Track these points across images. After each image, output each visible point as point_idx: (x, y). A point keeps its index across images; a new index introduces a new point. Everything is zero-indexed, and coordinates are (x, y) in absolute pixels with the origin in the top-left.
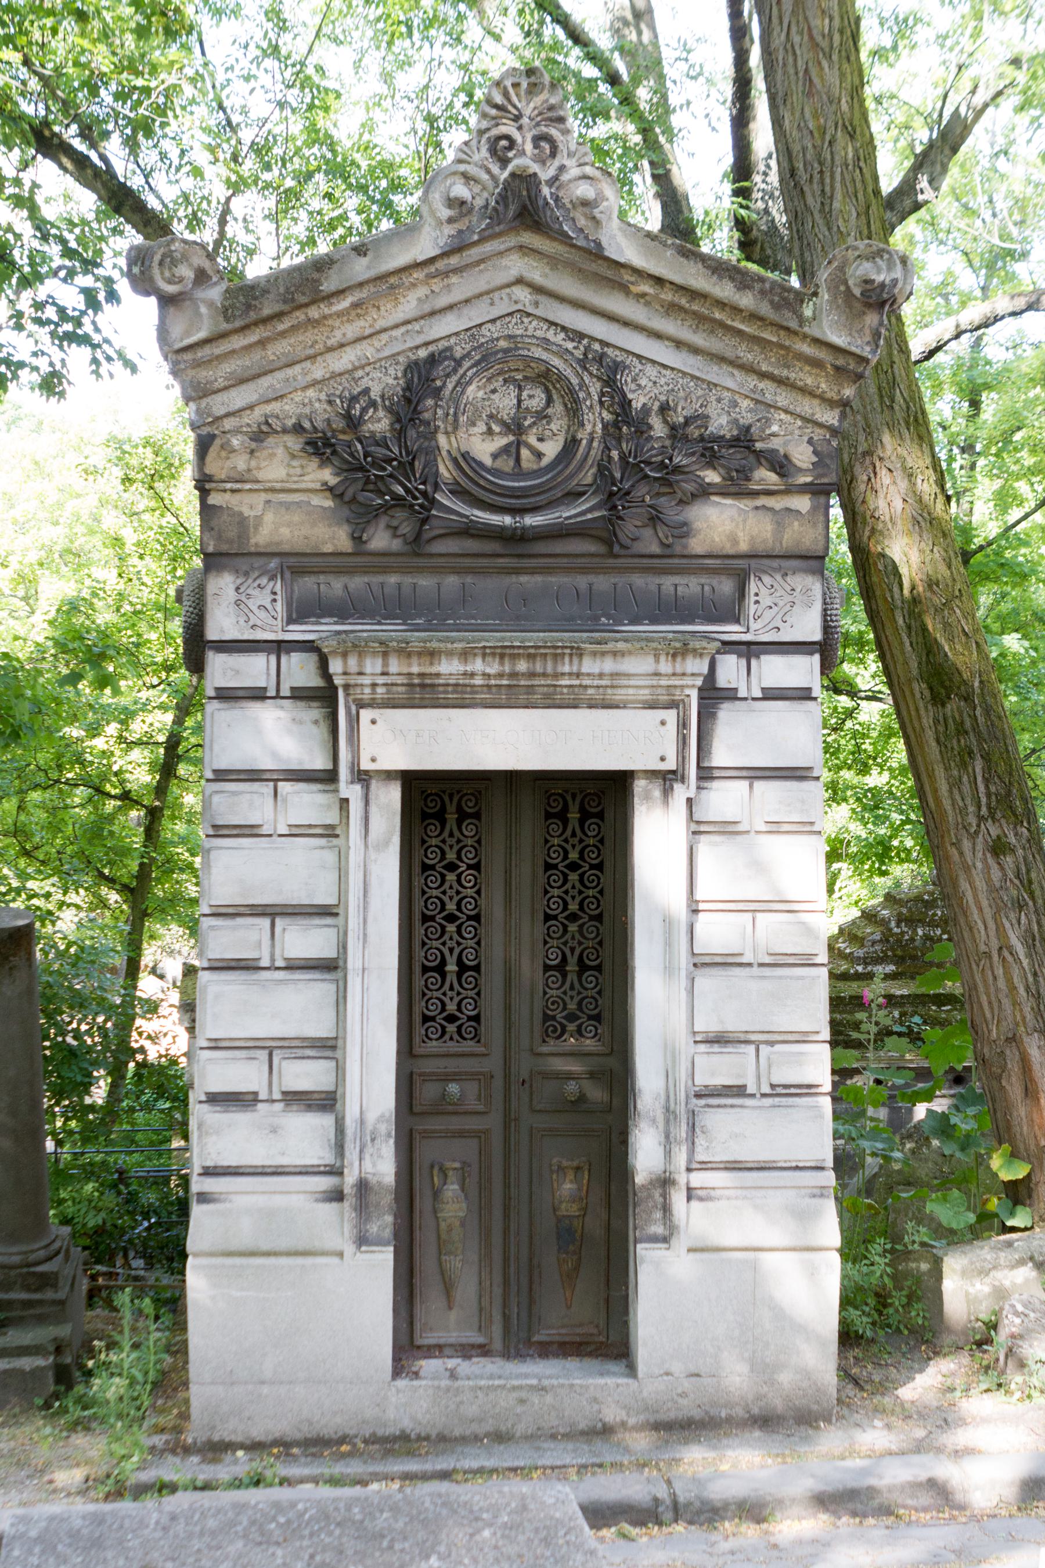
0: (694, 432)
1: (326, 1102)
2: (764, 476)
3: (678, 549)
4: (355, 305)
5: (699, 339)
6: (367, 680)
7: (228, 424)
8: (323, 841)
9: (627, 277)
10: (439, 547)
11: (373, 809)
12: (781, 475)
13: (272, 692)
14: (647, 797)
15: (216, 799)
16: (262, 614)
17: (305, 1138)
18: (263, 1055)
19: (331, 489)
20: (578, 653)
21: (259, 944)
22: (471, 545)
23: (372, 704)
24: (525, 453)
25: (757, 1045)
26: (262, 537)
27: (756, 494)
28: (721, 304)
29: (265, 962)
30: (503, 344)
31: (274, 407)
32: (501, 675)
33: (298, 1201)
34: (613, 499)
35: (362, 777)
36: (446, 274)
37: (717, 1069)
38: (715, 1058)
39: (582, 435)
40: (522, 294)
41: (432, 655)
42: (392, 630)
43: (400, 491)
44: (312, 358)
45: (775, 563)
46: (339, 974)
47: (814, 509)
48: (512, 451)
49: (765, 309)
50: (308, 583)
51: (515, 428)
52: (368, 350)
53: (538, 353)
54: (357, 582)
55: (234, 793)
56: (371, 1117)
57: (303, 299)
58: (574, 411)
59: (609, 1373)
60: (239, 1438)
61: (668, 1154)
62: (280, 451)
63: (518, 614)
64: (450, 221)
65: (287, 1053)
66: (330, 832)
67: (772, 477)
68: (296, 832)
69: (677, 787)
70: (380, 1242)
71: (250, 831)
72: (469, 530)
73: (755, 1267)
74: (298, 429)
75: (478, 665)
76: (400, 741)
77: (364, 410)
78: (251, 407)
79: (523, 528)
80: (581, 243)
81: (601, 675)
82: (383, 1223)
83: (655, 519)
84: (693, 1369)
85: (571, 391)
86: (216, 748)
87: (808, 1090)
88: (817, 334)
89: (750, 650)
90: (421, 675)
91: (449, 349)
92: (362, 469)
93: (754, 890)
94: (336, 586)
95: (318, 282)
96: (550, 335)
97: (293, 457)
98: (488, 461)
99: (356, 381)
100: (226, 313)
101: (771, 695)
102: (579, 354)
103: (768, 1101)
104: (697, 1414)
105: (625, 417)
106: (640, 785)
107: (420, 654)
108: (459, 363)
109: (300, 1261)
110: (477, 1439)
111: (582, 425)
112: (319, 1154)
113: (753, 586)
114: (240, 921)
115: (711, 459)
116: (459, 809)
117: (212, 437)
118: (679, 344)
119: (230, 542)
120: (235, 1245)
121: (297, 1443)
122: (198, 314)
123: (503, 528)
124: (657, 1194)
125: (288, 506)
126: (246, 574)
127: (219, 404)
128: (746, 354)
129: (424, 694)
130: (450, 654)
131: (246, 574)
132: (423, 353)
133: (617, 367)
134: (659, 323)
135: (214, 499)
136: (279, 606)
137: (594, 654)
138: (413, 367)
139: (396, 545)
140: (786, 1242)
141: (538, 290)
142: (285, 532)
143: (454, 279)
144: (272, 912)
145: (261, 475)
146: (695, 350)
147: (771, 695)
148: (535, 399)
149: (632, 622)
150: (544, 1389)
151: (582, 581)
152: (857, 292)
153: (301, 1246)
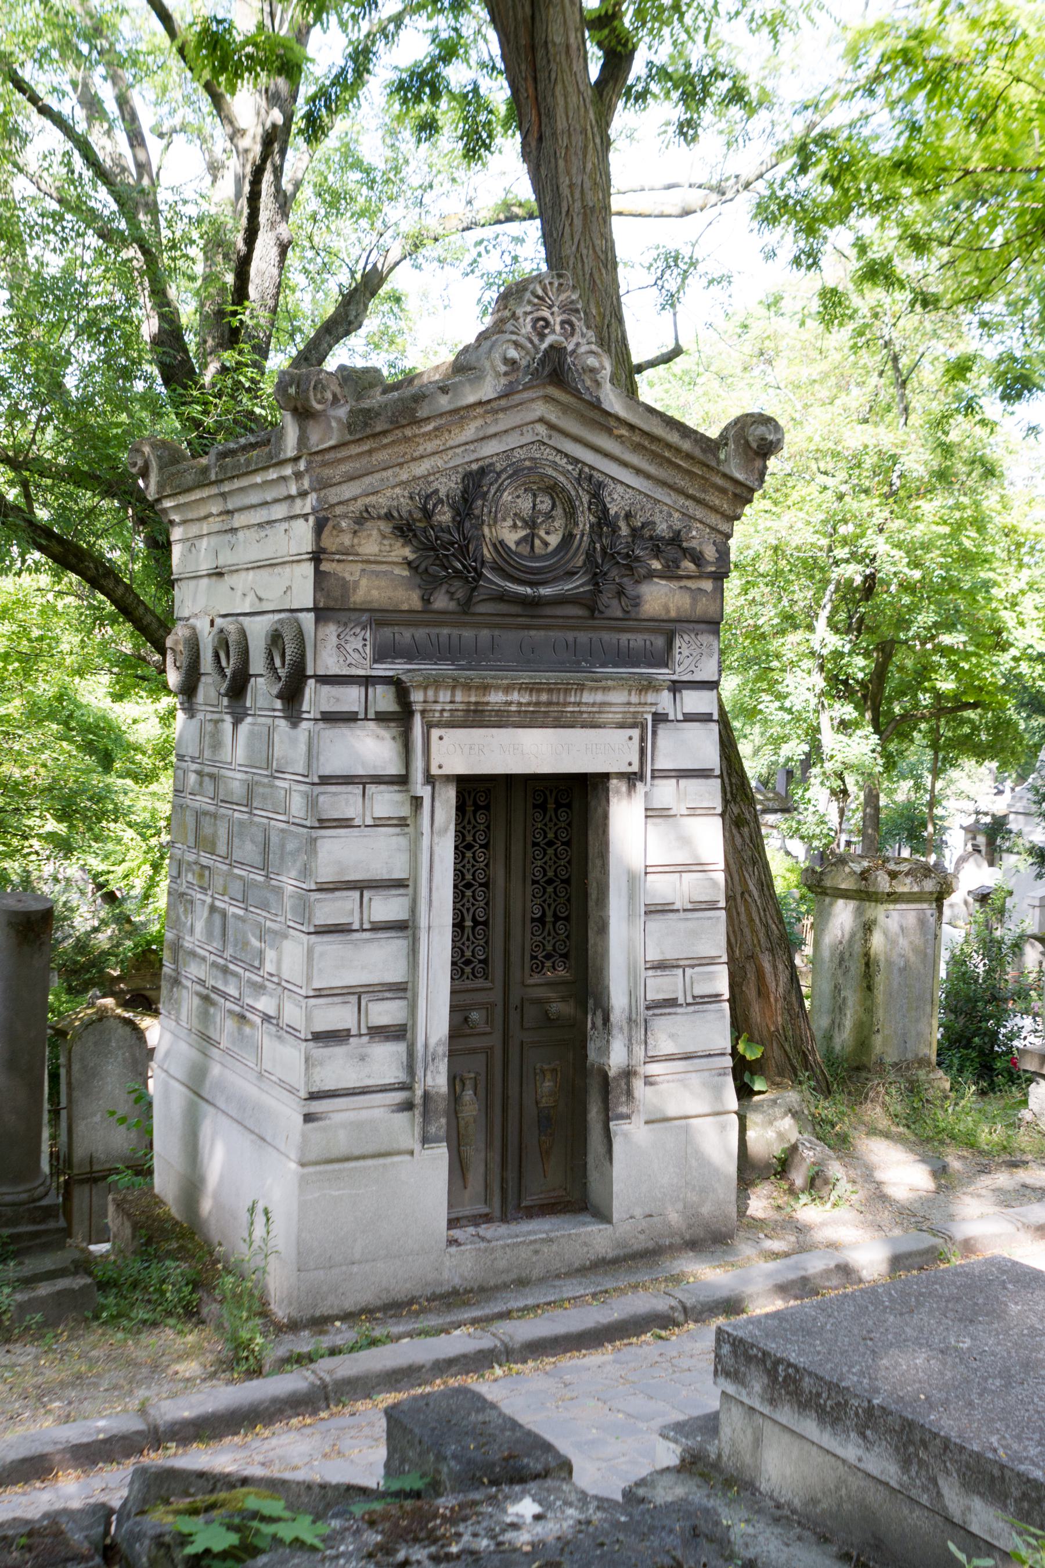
0: (647, 533)
1: (398, 1033)
2: (688, 565)
3: (633, 615)
4: (436, 429)
5: (652, 469)
6: (439, 707)
7: (338, 510)
8: (398, 830)
9: (613, 423)
10: (481, 608)
11: (437, 804)
12: (698, 565)
13: (361, 716)
14: (618, 792)
15: (321, 799)
16: (356, 655)
17: (384, 1062)
18: (354, 999)
19: (409, 564)
20: (581, 688)
21: (352, 912)
22: (503, 608)
23: (439, 725)
24: (537, 542)
25: (684, 968)
26: (358, 597)
27: (680, 578)
28: (669, 446)
29: (356, 926)
30: (527, 463)
31: (371, 500)
32: (529, 704)
33: (378, 1113)
34: (596, 578)
35: (430, 779)
36: (496, 412)
37: (659, 987)
38: (659, 980)
39: (577, 531)
40: (541, 429)
41: (485, 688)
42: (445, 668)
43: (459, 566)
44: (401, 465)
45: (691, 626)
46: (410, 932)
47: (715, 589)
48: (529, 540)
49: (697, 453)
50: (387, 632)
51: (531, 524)
52: (438, 462)
53: (550, 471)
54: (421, 633)
55: (335, 794)
56: (433, 1041)
57: (404, 422)
58: (571, 515)
59: (584, 1224)
60: (335, 1311)
61: (630, 1051)
62: (375, 532)
63: (528, 658)
64: (506, 374)
65: (371, 996)
66: (402, 823)
67: (691, 566)
68: (379, 823)
69: (639, 784)
70: (437, 1140)
71: (345, 823)
72: (503, 597)
73: (687, 1130)
74: (389, 516)
75: (515, 696)
76: (463, 752)
77: (435, 506)
78: (355, 499)
79: (540, 597)
80: (587, 397)
81: (594, 704)
82: (440, 1125)
83: (621, 593)
84: (648, 1212)
85: (570, 500)
86: (322, 758)
87: (716, 998)
88: (727, 471)
89: (676, 687)
90: (477, 703)
91: (492, 464)
92: (434, 549)
93: (681, 857)
94: (406, 636)
95: (415, 410)
96: (557, 459)
97: (384, 537)
98: (513, 547)
99: (430, 483)
100: (350, 427)
101: (689, 718)
102: (575, 474)
103: (691, 1009)
104: (650, 1245)
105: (604, 521)
106: (614, 783)
108: (499, 474)
109: (381, 1161)
110: (505, 1286)
111: (576, 524)
112: (393, 1074)
113: (677, 642)
114: (338, 894)
115: (657, 553)
116: (475, 804)
117: (327, 519)
118: (638, 471)
119: (336, 600)
120: (335, 1153)
121: (378, 1309)
122: (330, 427)
123: (526, 596)
124: (623, 1083)
125: (377, 574)
126: (345, 625)
127: (334, 495)
128: (681, 482)
129: (475, 717)
130: (497, 688)
131: (345, 625)
132: (474, 467)
133: (600, 485)
134: (634, 459)
135: (325, 567)
136: (368, 649)
138: (468, 476)
139: (452, 606)
140: (707, 1109)
141: (551, 426)
142: (375, 593)
143: (501, 415)
144: (361, 886)
145: (360, 550)
146: (648, 476)
147: (689, 718)
148: (545, 504)
149: (603, 666)
150: (551, 1240)
151: (570, 636)
152: (754, 445)
153: (383, 1148)
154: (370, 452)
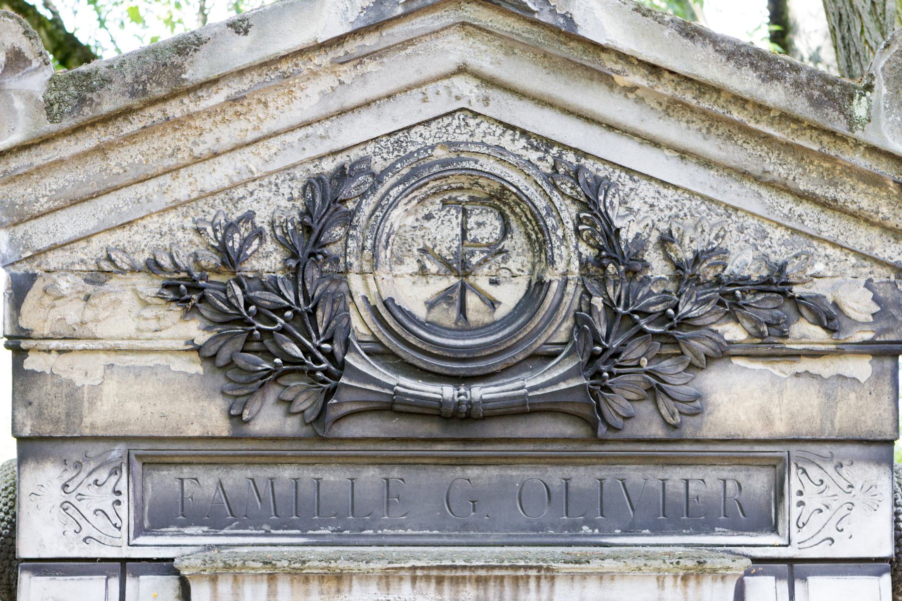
0: (707, 272)
2: (806, 332)
3: (688, 432)
4: (234, 100)
5: (711, 147)
7: (54, 260)
19: (198, 349)
24: (472, 300)
26: (99, 417)
28: (741, 101)
30: (440, 154)
31: (121, 237)
34: (598, 362)
36: (360, 60)
39: (553, 276)
40: (467, 88)
42: (284, 546)
43: (296, 351)
45: (825, 450)
47: (877, 375)
48: (456, 297)
49: (801, 107)
51: (459, 266)
52: (252, 161)
53: (489, 165)
58: (540, 243)
62: (128, 297)
72: (393, 406)
74: (153, 267)
77: (246, 242)
78: (87, 238)
83: (655, 390)
85: (536, 217)
91: (366, 160)
92: (241, 321)
97: (146, 304)
98: (421, 312)
99: (235, 202)
102: (546, 167)
105: (611, 253)
107: (322, 578)
108: (378, 179)
113: (794, 482)
118: (684, 154)
119: (56, 422)
123: (441, 403)
127: (41, 233)
128: (778, 168)
132: (329, 166)
133: (598, 185)
135: (32, 363)
137: (572, 576)
138: (314, 183)
139: (291, 426)
141: (489, 82)
142: (133, 409)
143: (371, 66)
145: (99, 331)
146: (707, 163)
148: (487, 227)
149: (627, 532)
151: (555, 476)
154: (101, 150)
